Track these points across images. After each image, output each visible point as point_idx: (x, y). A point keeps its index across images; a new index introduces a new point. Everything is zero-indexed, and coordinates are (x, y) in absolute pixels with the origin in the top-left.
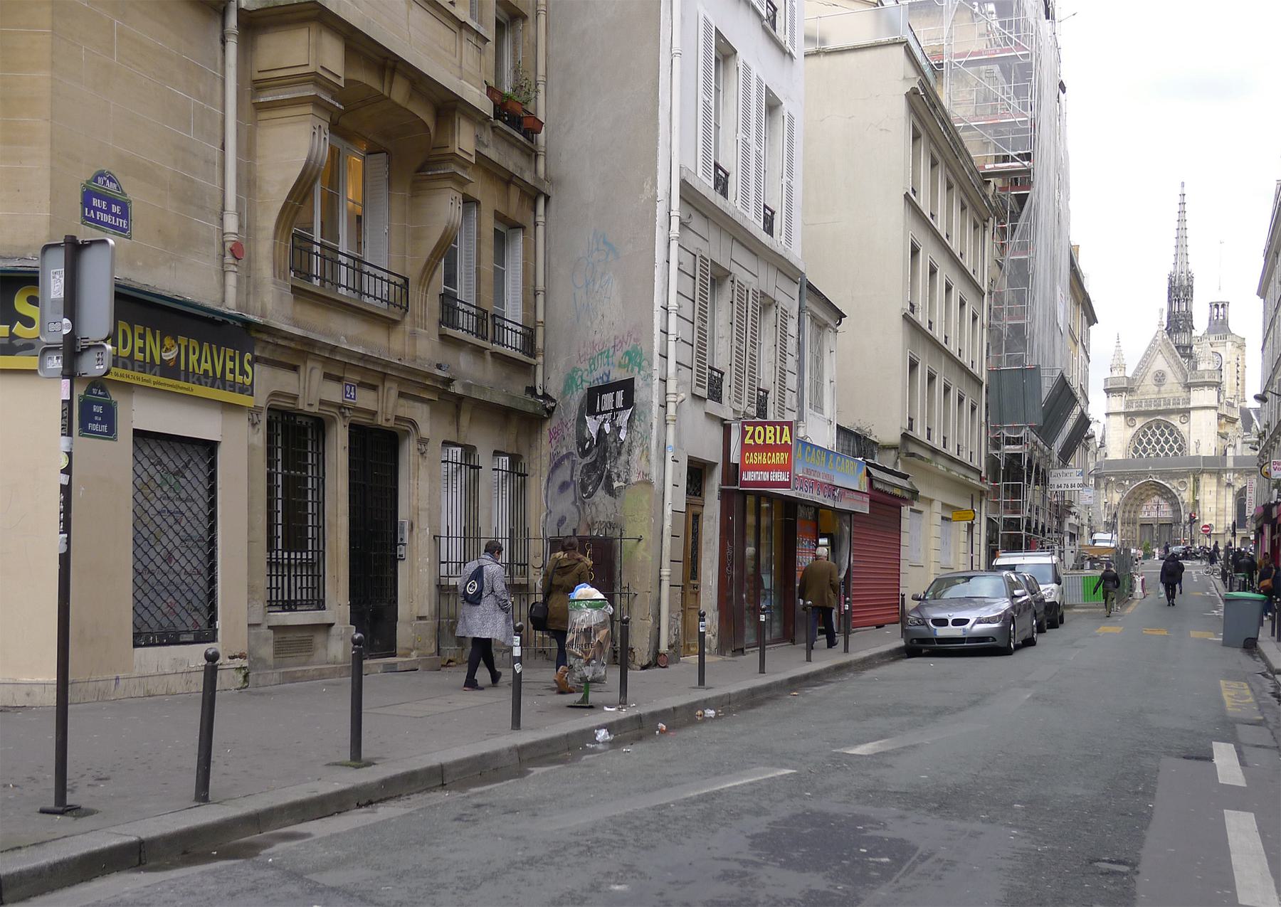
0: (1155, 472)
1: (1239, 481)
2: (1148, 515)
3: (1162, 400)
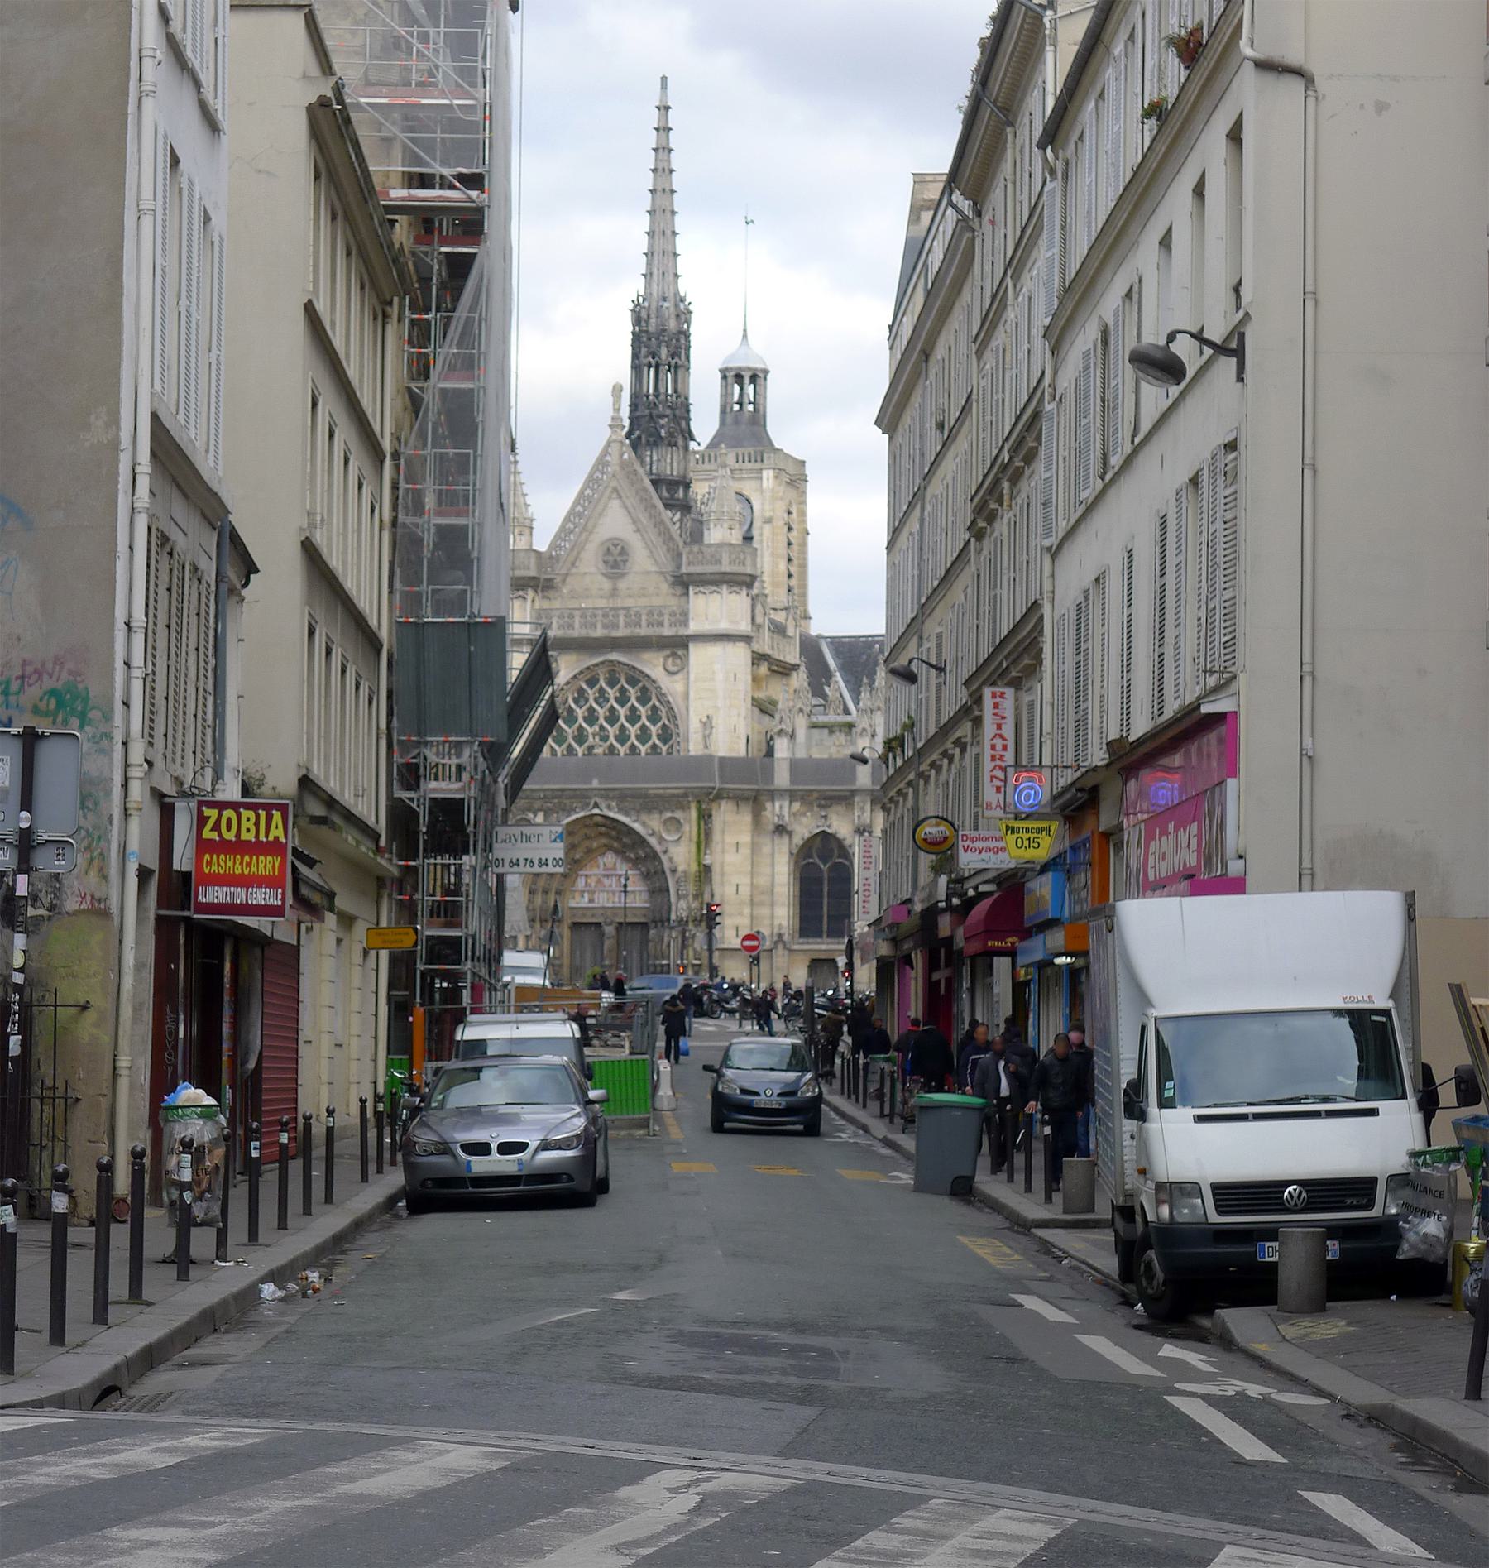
0: (606, 794)
1: (804, 820)
2: (591, 901)
3: (622, 613)
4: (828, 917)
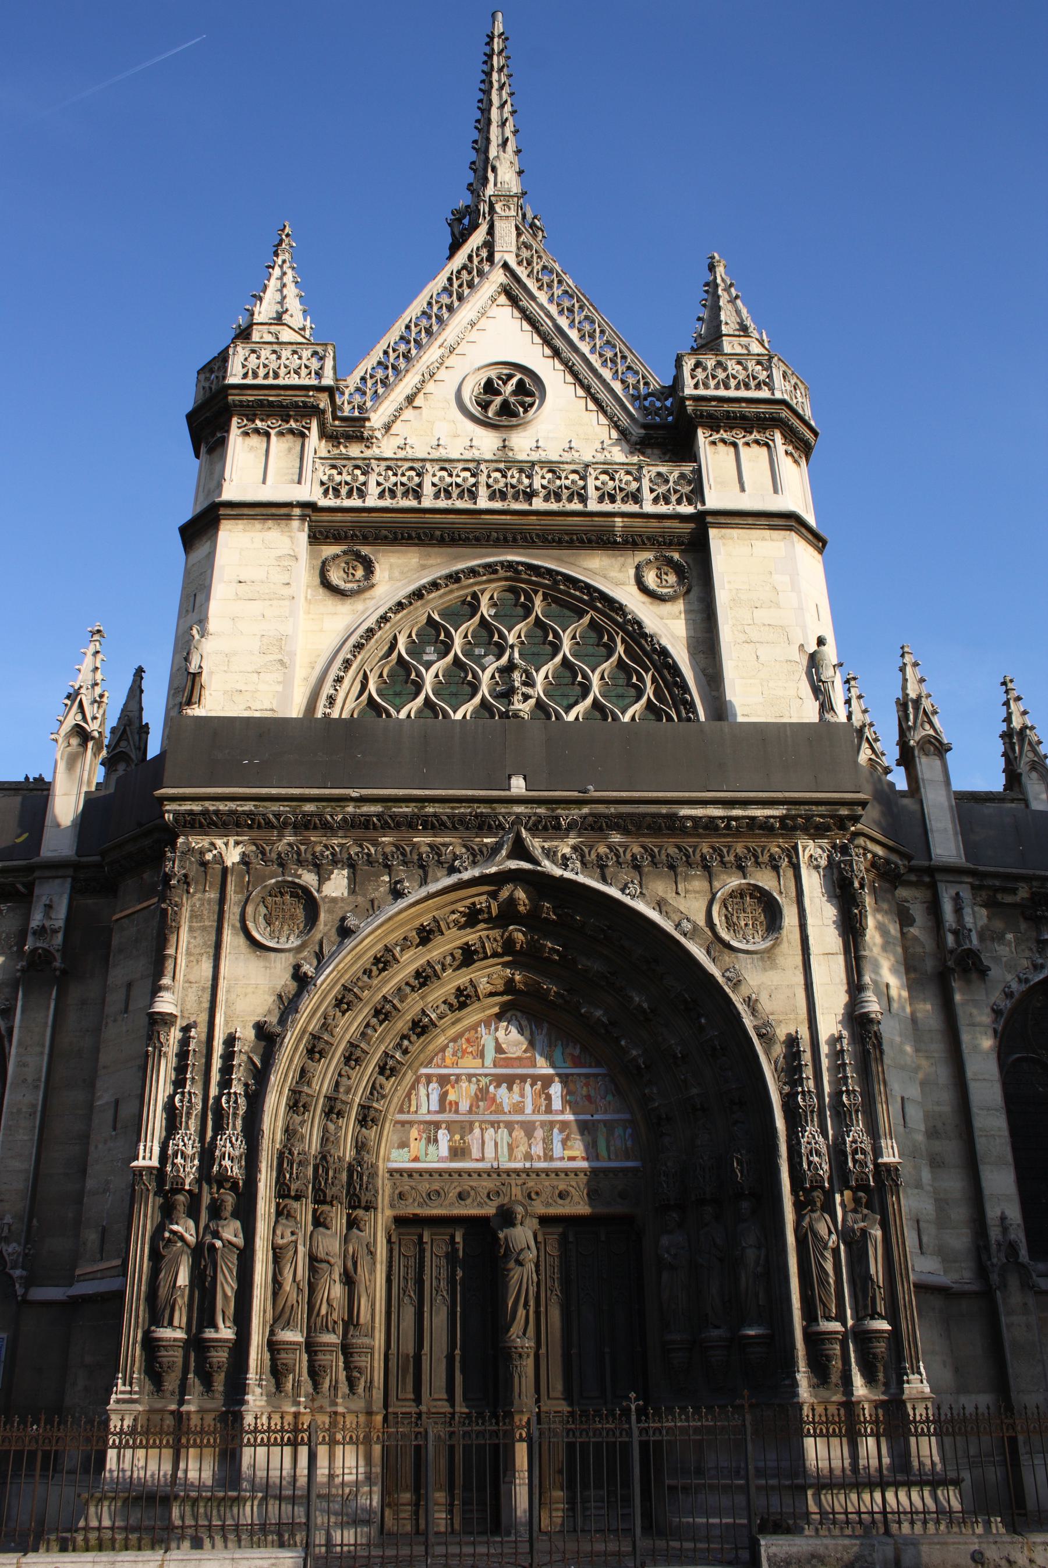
1: (1003, 951)
2: (458, 1152)
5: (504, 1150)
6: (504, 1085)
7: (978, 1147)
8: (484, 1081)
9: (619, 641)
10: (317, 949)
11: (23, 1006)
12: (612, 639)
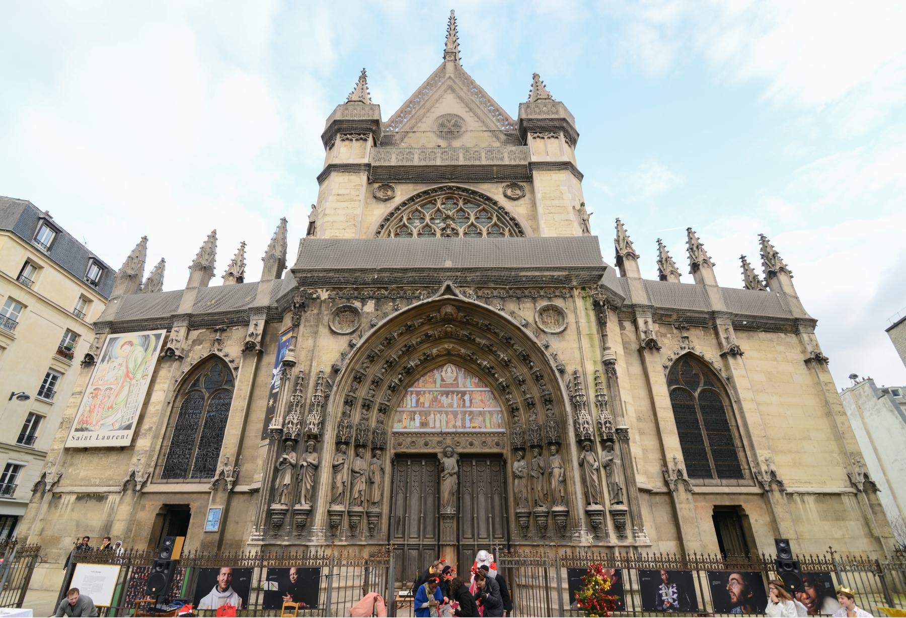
1: (666, 341)
2: (424, 424)
4: (714, 452)
5: (444, 423)
6: (445, 395)
7: (660, 426)
8: (436, 393)
9: (495, 215)
10: (360, 333)
11: (243, 365)
12: (492, 215)
